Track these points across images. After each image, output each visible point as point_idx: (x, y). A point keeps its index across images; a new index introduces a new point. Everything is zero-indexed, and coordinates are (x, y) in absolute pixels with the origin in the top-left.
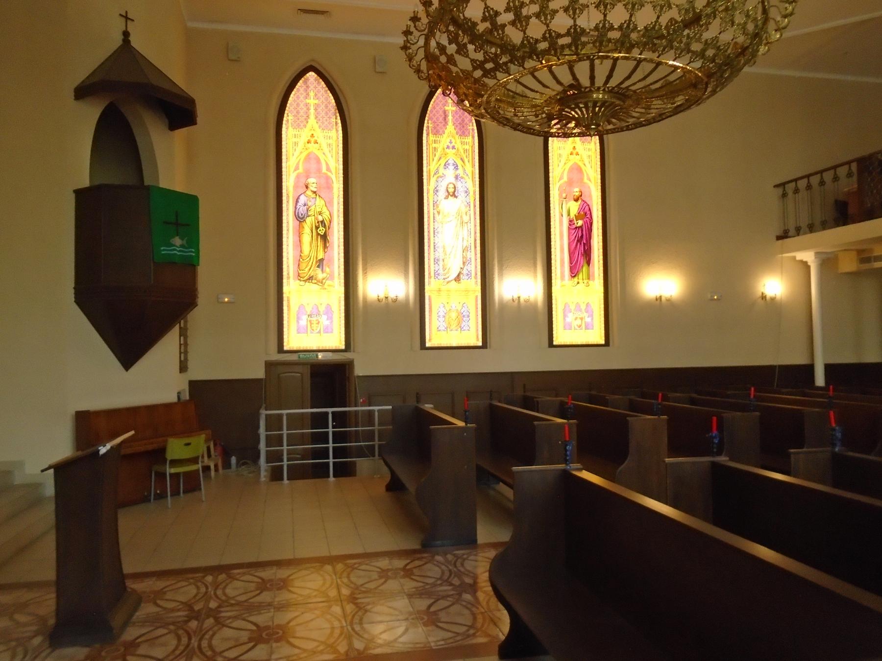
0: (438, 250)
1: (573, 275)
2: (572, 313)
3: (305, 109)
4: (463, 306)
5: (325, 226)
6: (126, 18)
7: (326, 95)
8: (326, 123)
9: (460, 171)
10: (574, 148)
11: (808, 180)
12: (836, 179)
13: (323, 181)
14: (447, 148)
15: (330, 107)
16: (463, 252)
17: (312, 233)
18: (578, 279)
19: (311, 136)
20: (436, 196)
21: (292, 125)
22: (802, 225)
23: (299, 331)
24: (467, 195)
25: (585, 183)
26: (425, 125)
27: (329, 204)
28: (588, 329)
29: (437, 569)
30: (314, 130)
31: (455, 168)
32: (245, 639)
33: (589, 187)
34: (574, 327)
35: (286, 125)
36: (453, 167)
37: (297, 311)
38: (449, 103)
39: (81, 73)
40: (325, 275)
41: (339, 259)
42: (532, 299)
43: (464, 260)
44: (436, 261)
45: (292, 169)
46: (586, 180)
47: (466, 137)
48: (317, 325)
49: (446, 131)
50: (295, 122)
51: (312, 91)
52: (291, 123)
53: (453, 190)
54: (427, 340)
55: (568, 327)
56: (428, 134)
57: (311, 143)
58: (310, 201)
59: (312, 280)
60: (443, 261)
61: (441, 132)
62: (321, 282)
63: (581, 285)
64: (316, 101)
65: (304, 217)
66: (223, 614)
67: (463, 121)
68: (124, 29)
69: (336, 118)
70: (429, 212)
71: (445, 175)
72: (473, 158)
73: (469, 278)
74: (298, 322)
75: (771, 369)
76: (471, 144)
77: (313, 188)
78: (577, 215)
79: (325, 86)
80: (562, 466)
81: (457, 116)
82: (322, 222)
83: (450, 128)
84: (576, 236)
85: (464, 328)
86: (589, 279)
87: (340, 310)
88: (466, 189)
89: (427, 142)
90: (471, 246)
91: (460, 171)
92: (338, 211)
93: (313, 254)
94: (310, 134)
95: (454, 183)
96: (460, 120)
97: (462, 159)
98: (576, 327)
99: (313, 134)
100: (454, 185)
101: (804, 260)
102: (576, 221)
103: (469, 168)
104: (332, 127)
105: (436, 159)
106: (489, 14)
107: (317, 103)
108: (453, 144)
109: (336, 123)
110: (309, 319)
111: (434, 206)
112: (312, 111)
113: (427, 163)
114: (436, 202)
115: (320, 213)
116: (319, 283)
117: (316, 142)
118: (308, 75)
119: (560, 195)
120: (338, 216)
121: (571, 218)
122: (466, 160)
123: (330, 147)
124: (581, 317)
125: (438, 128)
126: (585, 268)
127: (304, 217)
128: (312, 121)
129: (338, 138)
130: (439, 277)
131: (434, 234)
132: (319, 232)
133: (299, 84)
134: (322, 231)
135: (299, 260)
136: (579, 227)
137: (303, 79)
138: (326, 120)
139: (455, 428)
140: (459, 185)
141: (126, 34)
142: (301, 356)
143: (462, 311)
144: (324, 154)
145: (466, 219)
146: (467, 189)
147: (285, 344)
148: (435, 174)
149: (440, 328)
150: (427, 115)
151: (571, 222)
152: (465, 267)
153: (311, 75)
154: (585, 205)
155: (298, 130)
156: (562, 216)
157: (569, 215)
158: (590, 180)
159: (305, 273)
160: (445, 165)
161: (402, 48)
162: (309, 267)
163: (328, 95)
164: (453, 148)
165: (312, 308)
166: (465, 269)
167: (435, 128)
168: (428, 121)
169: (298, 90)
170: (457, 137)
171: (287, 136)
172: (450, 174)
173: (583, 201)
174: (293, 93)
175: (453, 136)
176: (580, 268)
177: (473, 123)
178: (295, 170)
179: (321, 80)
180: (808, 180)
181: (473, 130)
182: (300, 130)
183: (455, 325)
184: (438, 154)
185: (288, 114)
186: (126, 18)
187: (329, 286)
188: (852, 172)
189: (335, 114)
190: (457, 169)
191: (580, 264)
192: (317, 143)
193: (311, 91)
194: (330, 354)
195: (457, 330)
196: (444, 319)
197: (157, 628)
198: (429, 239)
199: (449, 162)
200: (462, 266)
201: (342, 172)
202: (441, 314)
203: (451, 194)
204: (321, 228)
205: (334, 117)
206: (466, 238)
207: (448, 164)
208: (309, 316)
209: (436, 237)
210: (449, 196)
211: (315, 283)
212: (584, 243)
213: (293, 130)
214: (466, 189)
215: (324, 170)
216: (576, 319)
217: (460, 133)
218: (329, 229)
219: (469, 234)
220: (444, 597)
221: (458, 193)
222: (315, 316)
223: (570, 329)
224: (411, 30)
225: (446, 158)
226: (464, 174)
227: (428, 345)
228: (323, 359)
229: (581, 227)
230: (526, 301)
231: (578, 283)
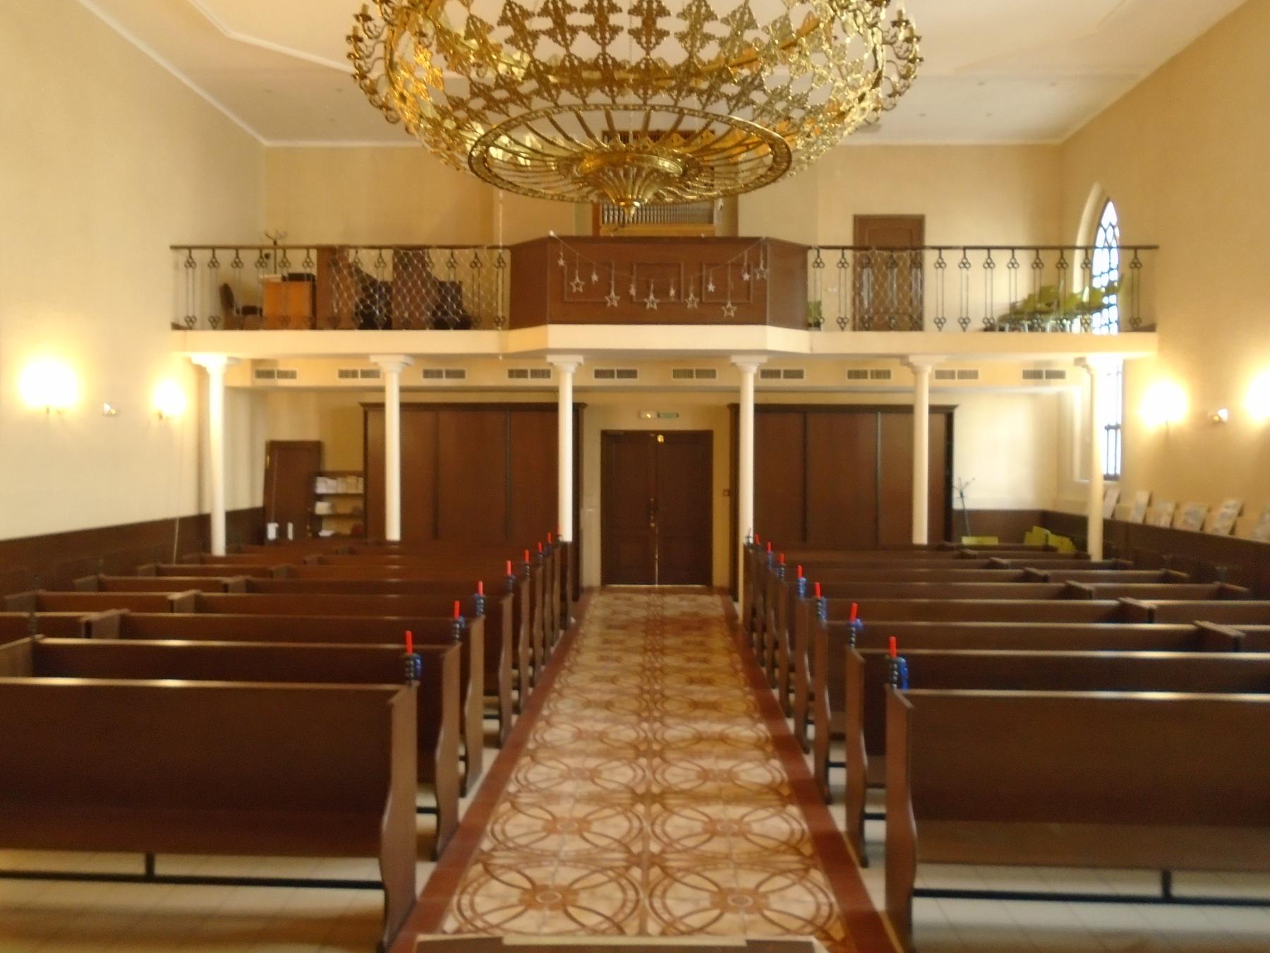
22: (198, 315)
101: (204, 365)
188: (311, 262)
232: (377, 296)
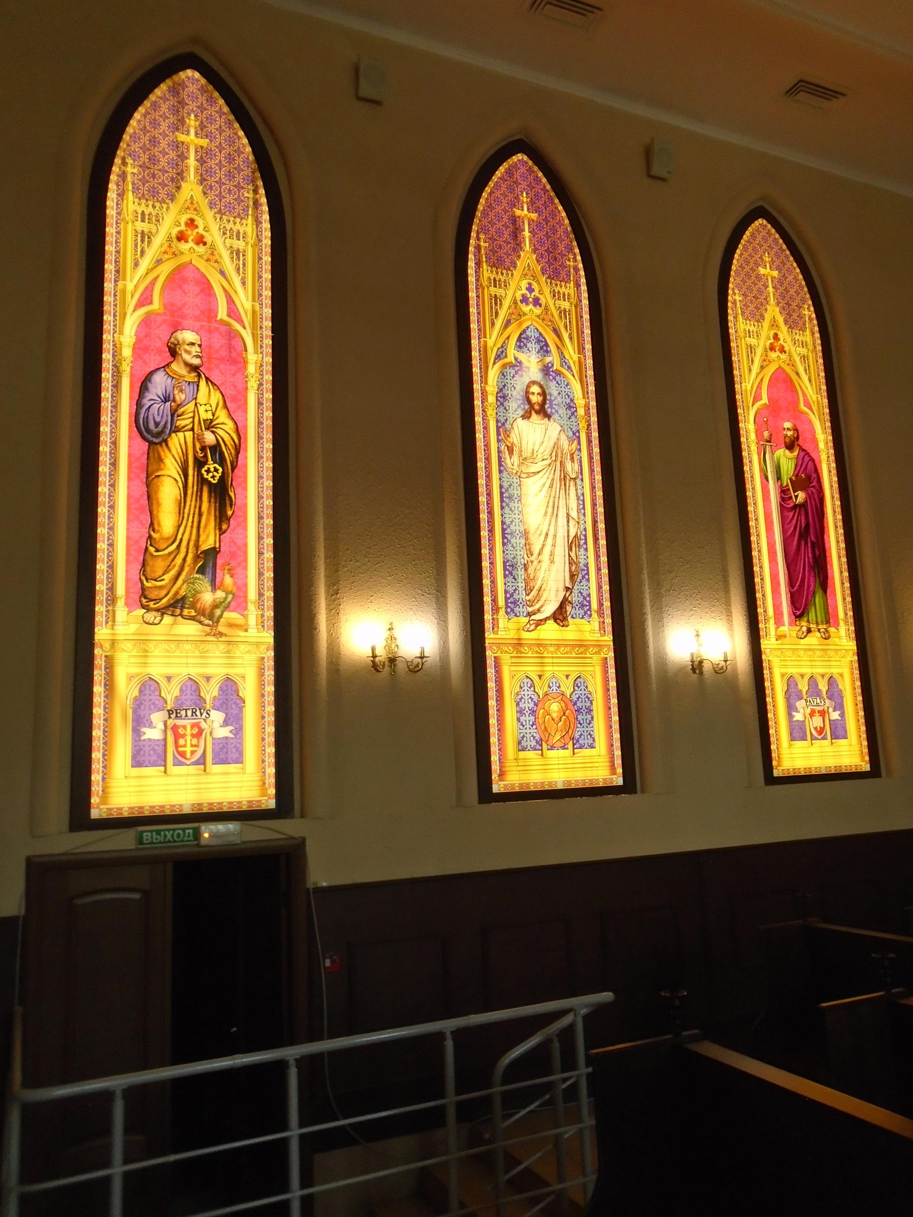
0: (513, 541)
1: (798, 613)
2: (803, 701)
3: (172, 155)
4: (576, 685)
5: (222, 462)
7: (228, 132)
8: (230, 198)
9: (553, 358)
10: (776, 337)
13: (218, 341)
14: (522, 301)
15: (239, 161)
16: (570, 549)
17: (186, 475)
18: (808, 621)
19: (187, 224)
20: (502, 409)
21: (136, 189)
23: (138, 761)
25: (802, 413)
26: (472, 242)
28: (837, 738)
30: (195, 209)
31: (541, 348)
33: (810, 422)
35: (118, 185)
36: (538, 347)
37: (135, 699)
38: (523, 202)
40: (220, 594)
43: (573, 568)
45: (132, 303)
47: (563, 284)
48: (195, 741)
49: (518, 263)
50: (144, 181)
52: (133, 183)
53: (540, 399)
54: (494, 777)
55: (798, 732)
56: (478, 264)
57: (186, 241)
58: (181, 391)
59: (182, 608)
60: (526, 570)
63: (814, 640)
64: (204, 142)
65: (162, 432)
69: (255, 191)
70: (487, 446)
71: (520, 363)
72: (580, 333)
74: (137, 732)
79: (226, 109)
81: (541, 234)
82: (216, 449)
83: (527, 257)
85: (581, 742)
86: (828, 622)
87: (263, 696)
88: (568, 401)
89: (477, 280)
90: (585, 536)
91: (553, 358)
92: (260, 423)
93: (186, 535)
94: (184, 218)
95: (542, 383)
97: (556, 332)
100: (541, 386)
102: (794, 492)
104: (245, 210)
105: (499, 323)
107: (205, 145)
109: (256, 204)
110: (170, 723)
111: (498, 434)
112: (192, 162)
114: (503, 424)
115: (210, 425)
116: (202, 619)
117: (200, 241)
118: (182, 75)
119: (759, 433)
120: (259, 438)
121: (785, 484)
122: (565, 336)
123: (239, 259)
124: (821, 708)
125: (501, 253)
126: (818, 599)
127: (162, 432)
128: (191, 188)
129: (260, 241)
130: (516, 610)
131: (502, 501)
132: (209, 477)
133: (158, 92)
134: (213, 472)
135: (147, 548)
137: (169, 82)
138: (230, 191)
140: (553, 389)
142: (146, 836)
143: (574, 698)
144: (222, 273)
146: (572, 400)
148: (498, 357)
149: (524, 744)
150: (476, 221)
152: (576, 587)
154: (807, 459)
155: (150, 203)
158: (811, 409)
159: (161, 587)
160: (519, 339)
162: (173, 573)
163: (236, 134)
164: (536, 302)
165: (181, 690)
166: (575, 591)
167: (493, 251)
168: (478, 233)
169: (155, 106)
170: (543, 279)
171: (119, 214)
172: (532, 363)
173: (803, 450)
174: (141, 109)
175: (534, 277)
176: (810, 598)
177: (575, 255)
178: (140, 304)
179: (216, 94)
181: (576, 269)
182: (158, 205)
183: (558, 737)
184: (503, 313)
185: (123, 159)
187: (231, 625)
190: (547, 352)
191: (809, 586)
192: (205, 244)
193: (189, 115)
195: (564, 748)
196: (532, 718)
198: (491, 513)
199: (528, 333)
201: (269, 324)
202: (527, 705)
204: (211, 466)
205: (251, 187)
206: (574, 514)
208: (170, 712)
209: (507, 510)
210: (533, 412)
211: (192, 618)
212: (813, 543)
213: (137, 200)
214: (568, 401)
215: (222, 313)
216: (812, 714)
217: (550, 271)
218: (233, 470)
219: (581, 506)
221: (551, 407)
222: (189, 713)
223: (804, 738)
225: (520, 324)
226: (562, 366)
227: (497, 787)
228: (214, 842)
229: (803, 506)
230: (718, 671)
231: (809, 631)
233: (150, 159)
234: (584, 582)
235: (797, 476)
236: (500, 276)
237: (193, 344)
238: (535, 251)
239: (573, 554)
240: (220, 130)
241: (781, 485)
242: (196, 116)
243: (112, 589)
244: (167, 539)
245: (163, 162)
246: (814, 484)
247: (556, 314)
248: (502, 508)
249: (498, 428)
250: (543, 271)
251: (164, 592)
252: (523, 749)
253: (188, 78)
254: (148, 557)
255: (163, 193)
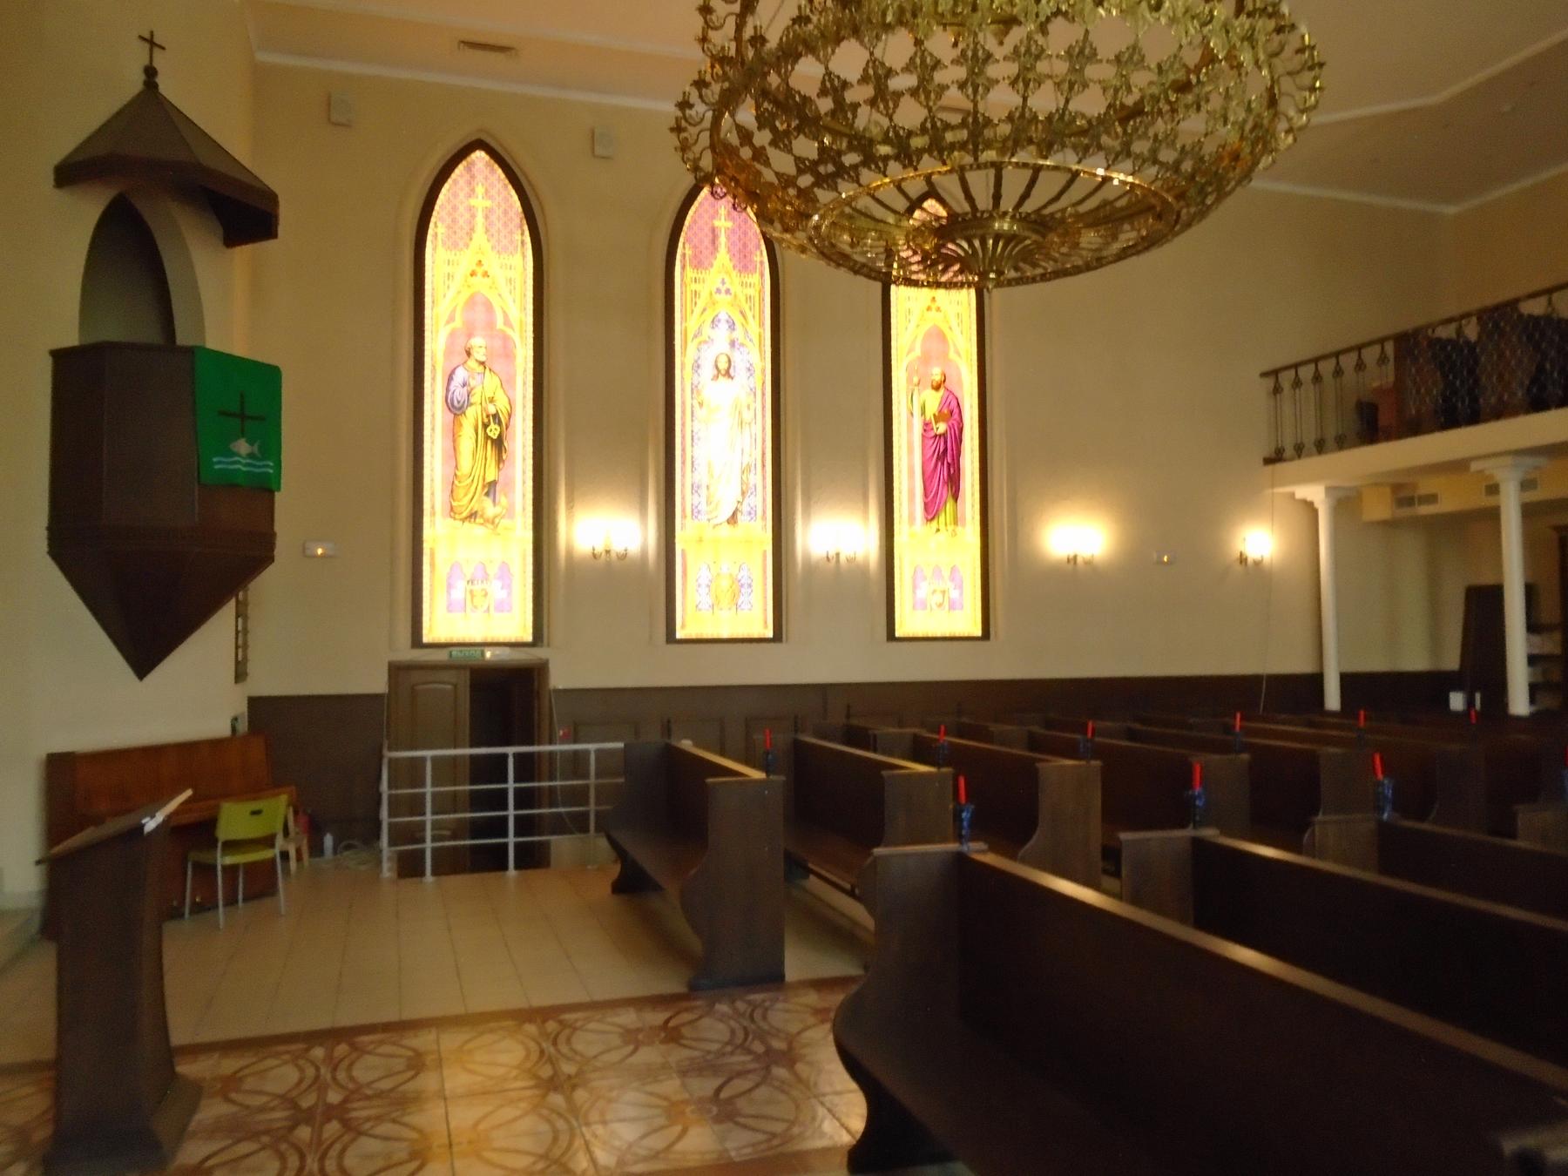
1: (929, 517)
3: (467, 216)
5: (500, 423)
6: (151, 42)
7: (505, 193)
9: (738, 334)
11: (1316, 366)
12: (1360, 366)
13: (498, 343)
14: (716, 293)
16: (743, 472)
19: (477, 264)
21: (444, 243)
22: (1306, 441)
23: (450, 608)
24: (751, 375)
27: (507, 383)
29: (721, 1026)
32: (403, 1155)
33: (958, 368)
34: (931, 606)
39: (65, 142)
40: (498, 510)
41: (524, 483)
42: (860, 556)
44: (695, 488)
46: (952, 355)
50: (449, 237)
51: (480, 184)
52: (442, 240)
53: (726, 366)
55: (919, 605)
56: (683, 267)
59: (475, 519)
61: (706, 264)
62: (492, 522)
64: (488, 203)
65: (462, 406)
66: (354, 1114)
67: (745, 245)
68: (147, 62)
69: (522, 234)
72: (762, 312)
73: (752, 519)
74: (449, 593)
75: (1254, 680)
76: (758, 288)
77: (479, 354)
78: (937, 414)
79: (503, 176)
80: (952, 847)
81: (735, 238)
82: (496, 416)
83: (723, 257)
84: (935, 451)
88: (748, 365)
89: (682, 280)
91: (738, 334)
92: (524, 397)
93: (478, 471)
95: (729, 354)
96: (740, 245)
97: (742, 313)
98: (934, 606)
99: (480, 261)
101: (1309, 499)
103: (753, 327)
105: (698, 310)
106: (832, 84)
108: (727, 285)
109: (523, 243)
110: (470, 587)
111: (692, 393)
112: (480, 220)
113: (682, 318)
117: (486, 274)
119: (909, 380)
122: (749, 315)
126: (950, 505)
127: (462, 406)
128: (480, 236)
134: (494, 431)
135: (453, 482)
136: (940, 436)
139: (741, 783)
140: (737, 358)
141: (150, 72)
142: (454, 653)
144: (500, 295)
145: (748, 416)
147: (425, 632)
148: (695, 336)
150: (683, 234)
151: (927, 426)
153: (479, 156)
154: (951, 397)
156: (912, 414)
157: (923, 412)
159: (463, 506)
160: (713, 322)
161: (672, 130)
162: (470, 496)
163: (509, 194)
164: (728, 291)
167: (695, 256)
168: (684, 244)
169: (455, 182)
170: (734, 273)
172: (721, 335)
174: (446, 186)
175: (727, 272)
176: (941, 505)
177: (761, 251)
179: (496, 166)
180: (1316, 366)
181: (762, 263)
184: (701, 303)
186: (151, 42)
189: (521, 226)
193: (477, 184)
194: (507, 650)
197: (239, 1141)
198: (683, 450)
199: (720, 316)
200: (740, 499)
202: (704, 582)
203: (723, 372)
205: (520, 232)
207: (719, 321)
208: (468, 582)
211: (482, 524)
212: (948, 463)
214: (748, 365)
215: (500, 324)
216: (934, 592)
220: (741, 1074)
224: (691, 101)
227: (680, 634)
228: (493, 659)
229: (944, 435)
231: (938, 530)
232: (1458, 383)
233: (452, 221)
234: (752, 497)
235: (940, 412)
236: (700, 275)
237: (481, 347)
238: (729, 251)
239: (744, 478)
240: (499, 193)
241: (925, 419)
242: (483, 185)
243: (433, 507)
244: (465, 475)
245: (461, 222)
246: (956, 416)
247: (743, 299)
248: (692, 446)
249: (692, 389)
250: (734, 267)
251: (464, 509)
252: (700, 610)
253: (477, 157)
254: (454, 487)
255: (461, 244)
